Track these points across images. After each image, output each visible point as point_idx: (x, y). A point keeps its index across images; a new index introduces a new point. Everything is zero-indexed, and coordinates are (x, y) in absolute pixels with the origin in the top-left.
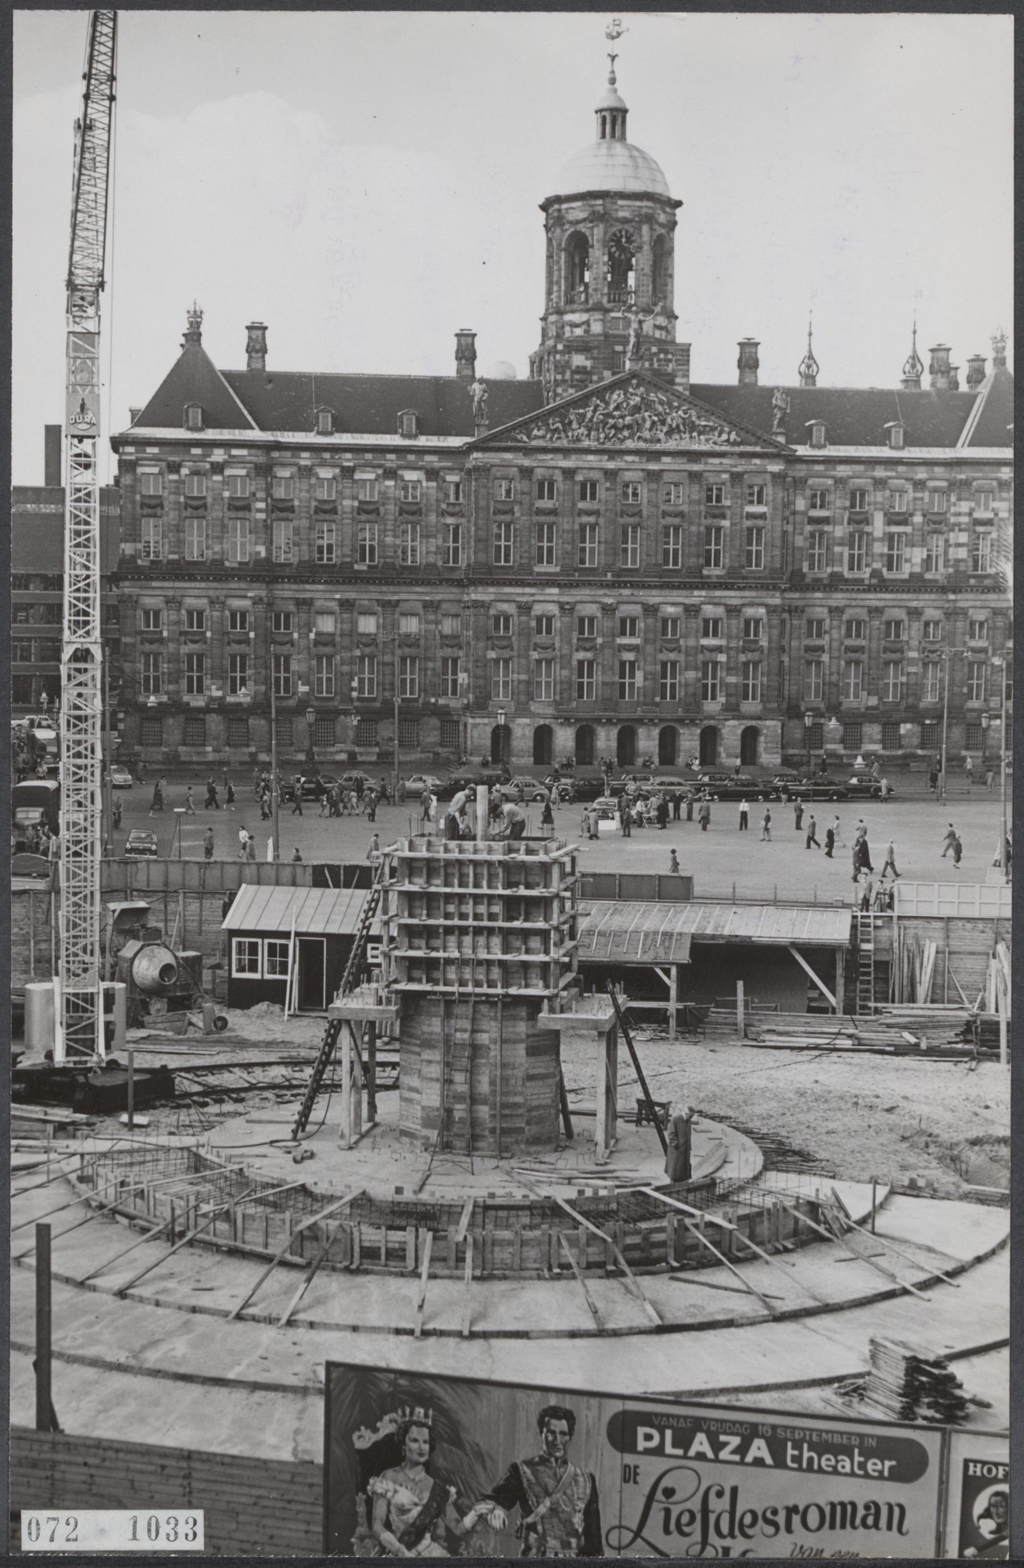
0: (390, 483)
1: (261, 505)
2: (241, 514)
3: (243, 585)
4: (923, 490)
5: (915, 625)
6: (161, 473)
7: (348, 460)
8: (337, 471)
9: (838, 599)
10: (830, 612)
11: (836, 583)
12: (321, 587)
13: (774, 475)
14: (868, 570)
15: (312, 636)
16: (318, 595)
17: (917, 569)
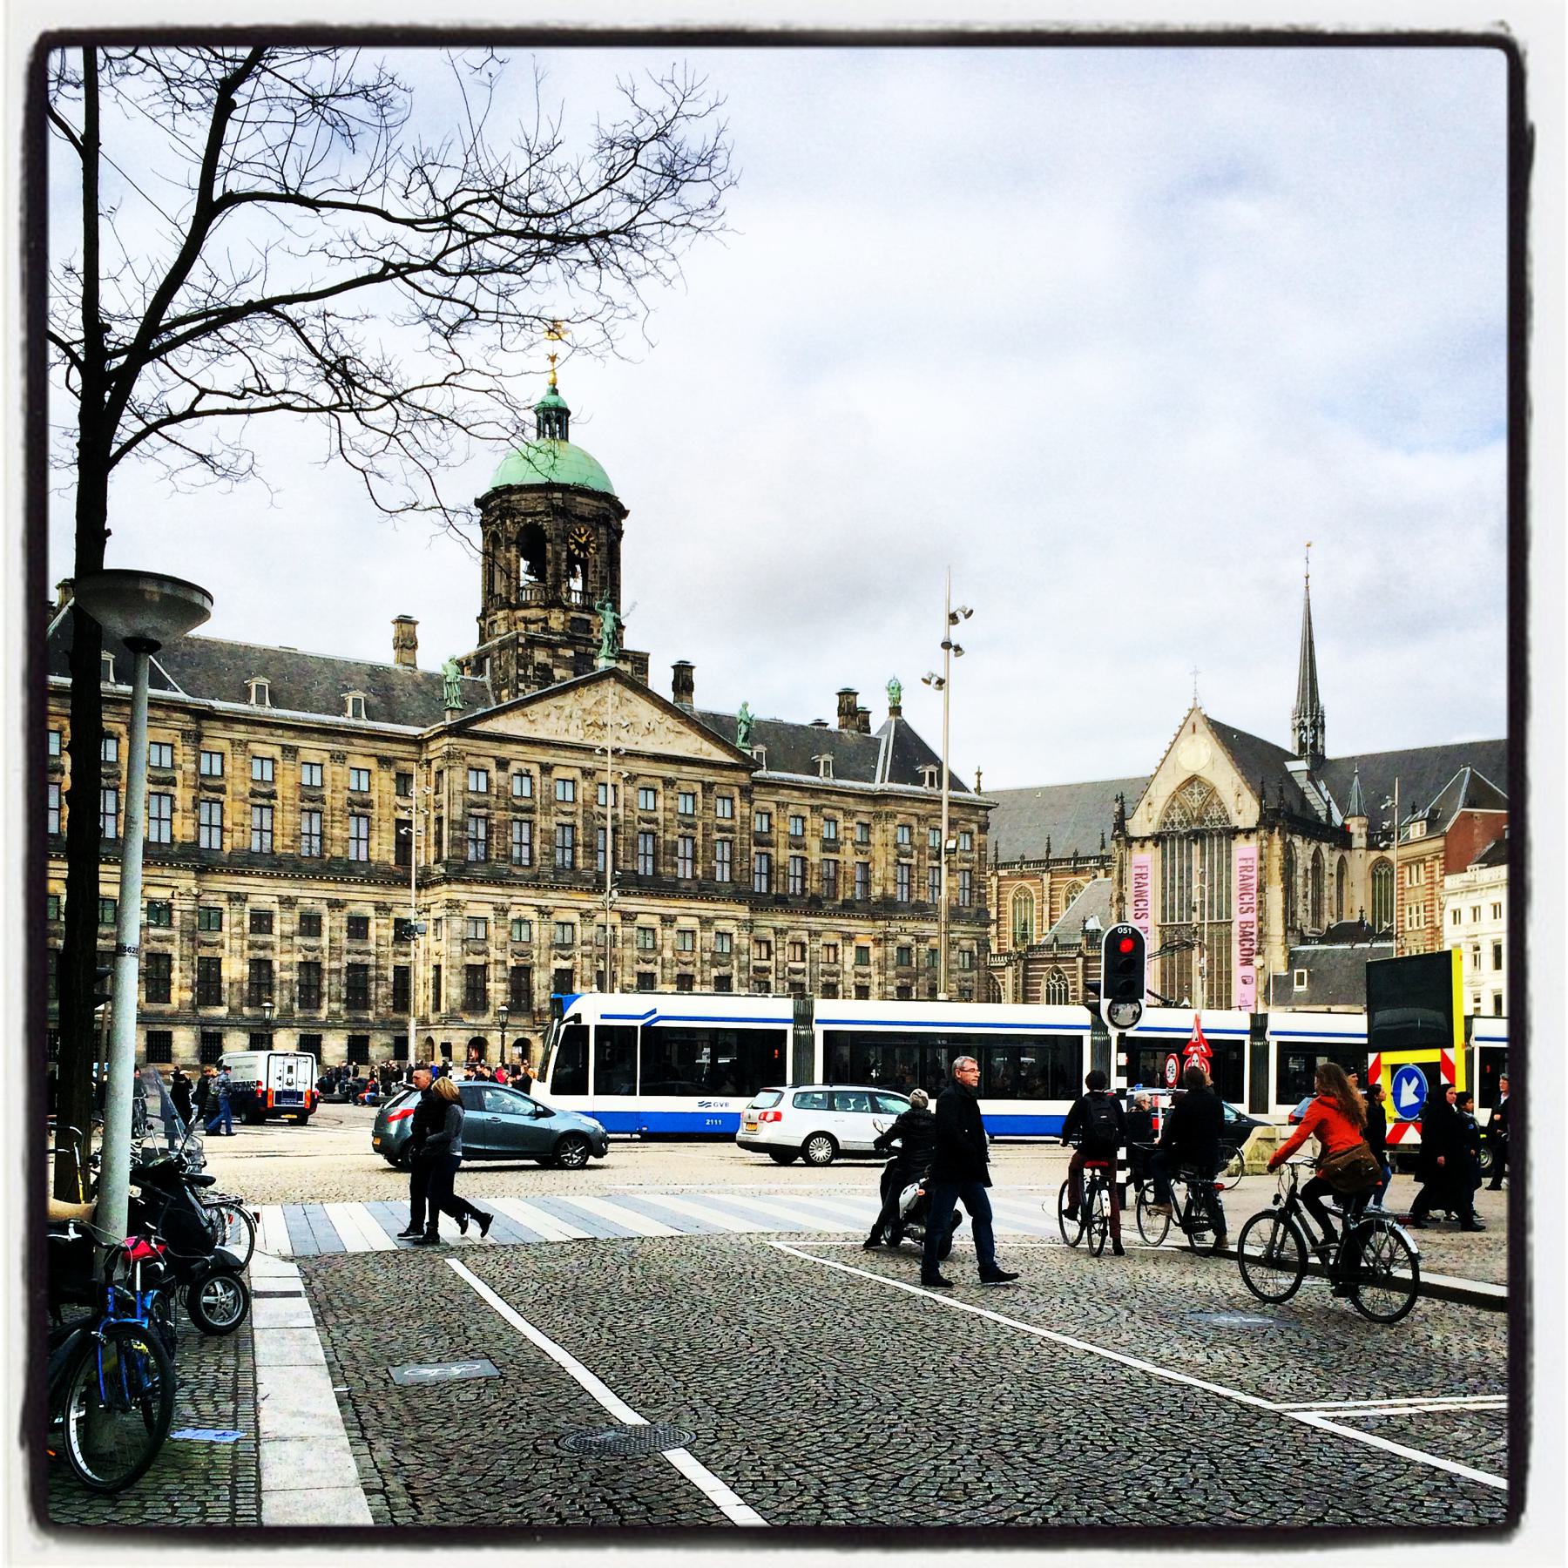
0: (339, 769)
3: (166, 872)
7: (289, 739)
9: (781, 921)
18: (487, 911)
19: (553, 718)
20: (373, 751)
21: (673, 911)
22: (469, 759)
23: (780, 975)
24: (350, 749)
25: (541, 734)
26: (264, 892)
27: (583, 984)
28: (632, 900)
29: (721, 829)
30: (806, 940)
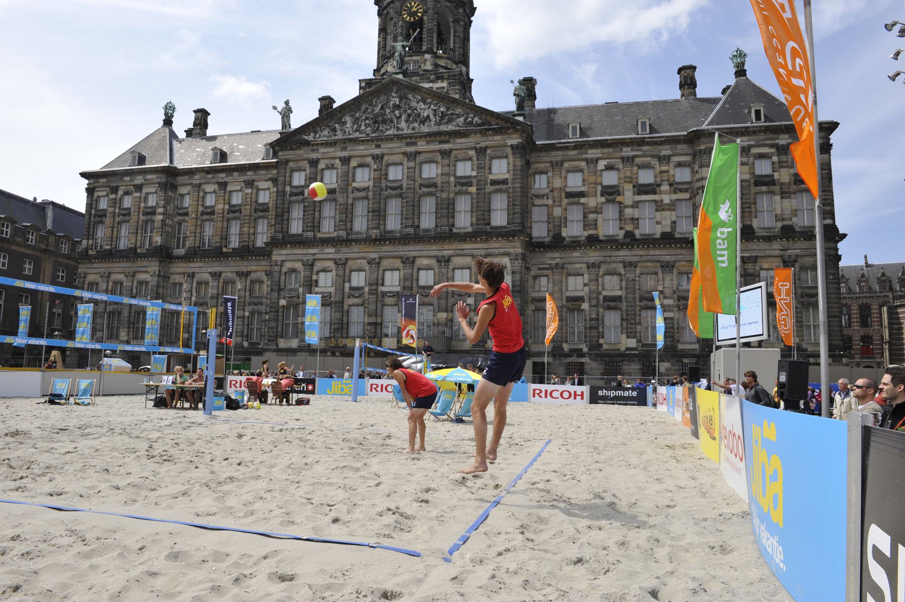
0: (249, 191)
1: (160, 210)
2: (149, 217)
3: (145, 264)
4: (668, 163)
5: (668, 278)
6: (107, 196)
8: (216, 187)
9: (594, 256)
10: (588, 268)
11: (593, 241)
12: (201, 265)
13: (512, 147)
14: (622, 233)
15: (194, 299)
16: (197, 270)
17: (668, 229)
18: (298, 265)
19: (349, 125)
20: (269, 176)
21: (446, 253)
22: (291, 164)
23: (594, 302)
24: (255, 177)
25: (340, 136)
26: (203, 270)
27: (369, 316)
28: (411, 248)
29: (494, 182)
30: (622, 271)
